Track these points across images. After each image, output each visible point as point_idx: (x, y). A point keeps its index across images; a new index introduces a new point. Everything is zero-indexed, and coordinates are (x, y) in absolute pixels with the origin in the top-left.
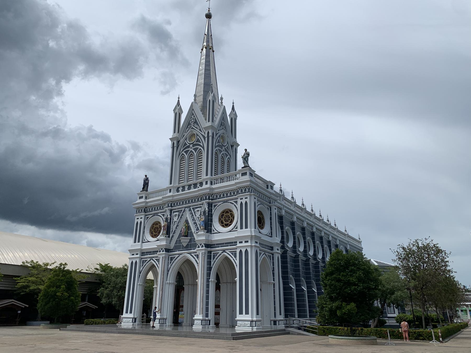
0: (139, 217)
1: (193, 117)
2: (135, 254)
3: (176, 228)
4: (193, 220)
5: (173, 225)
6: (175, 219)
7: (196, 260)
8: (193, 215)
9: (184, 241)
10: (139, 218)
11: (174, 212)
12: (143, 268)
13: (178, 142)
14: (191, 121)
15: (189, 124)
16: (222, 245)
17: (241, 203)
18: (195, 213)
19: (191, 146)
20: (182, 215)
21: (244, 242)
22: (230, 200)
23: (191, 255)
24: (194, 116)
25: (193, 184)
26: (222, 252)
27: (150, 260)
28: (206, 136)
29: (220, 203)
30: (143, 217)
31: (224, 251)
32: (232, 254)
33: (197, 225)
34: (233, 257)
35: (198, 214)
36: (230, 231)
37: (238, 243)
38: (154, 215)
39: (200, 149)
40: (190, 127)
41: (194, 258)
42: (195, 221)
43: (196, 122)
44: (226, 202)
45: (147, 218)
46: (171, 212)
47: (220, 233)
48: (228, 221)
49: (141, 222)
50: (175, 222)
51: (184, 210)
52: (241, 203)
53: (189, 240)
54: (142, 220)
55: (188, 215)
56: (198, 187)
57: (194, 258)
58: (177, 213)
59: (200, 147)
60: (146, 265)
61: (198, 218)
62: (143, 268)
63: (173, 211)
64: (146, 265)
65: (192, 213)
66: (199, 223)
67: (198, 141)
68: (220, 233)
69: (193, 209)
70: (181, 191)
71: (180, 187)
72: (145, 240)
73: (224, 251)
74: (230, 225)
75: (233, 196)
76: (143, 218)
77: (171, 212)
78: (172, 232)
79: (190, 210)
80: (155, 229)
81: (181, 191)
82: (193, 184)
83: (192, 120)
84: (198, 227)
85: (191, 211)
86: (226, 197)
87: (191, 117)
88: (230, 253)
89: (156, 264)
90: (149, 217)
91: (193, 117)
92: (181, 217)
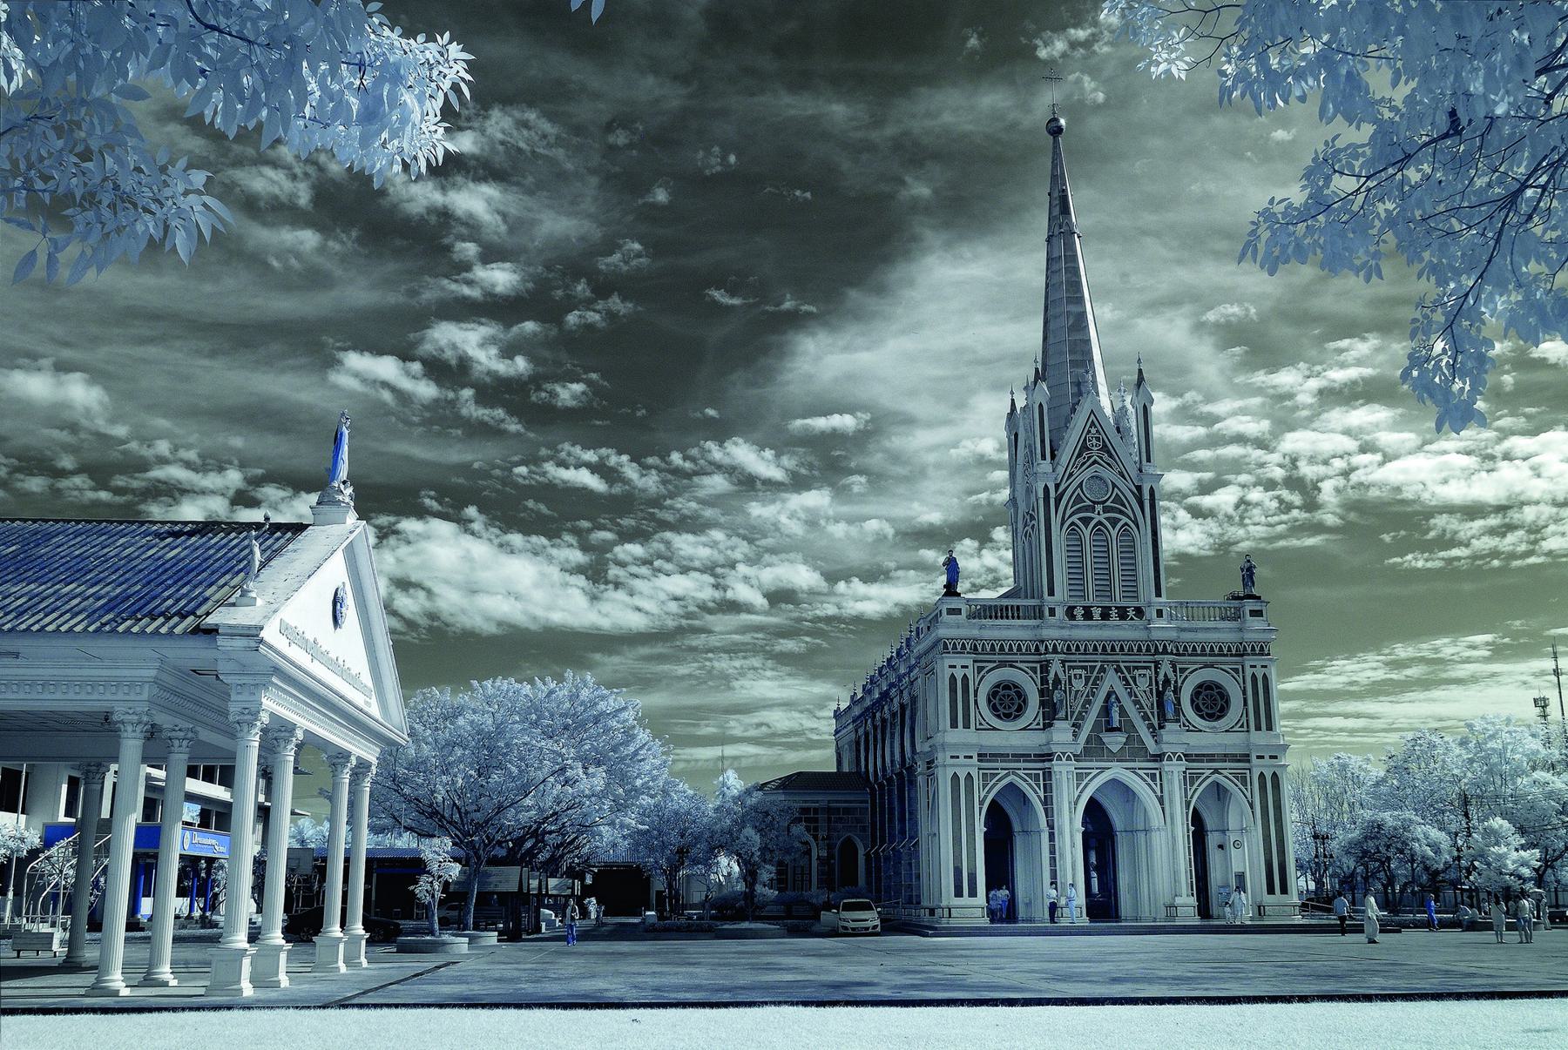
0: (959, 662)
1: (1093, 430)
2: (962, 758)
3: (1083, 706)
4: (1130, 694)
5: (1073, 697)
6: (1078, 685)
7: (1149, 785)
8: (1128, 683)
9: (1115, 741)
10: (959, 667)
11: (1070, 667)
12: (988, 792)
13: (1057, 486)
14: (1090, 441)
15: (1085, 448)
16: (1211, 758)
17: (1254, 677)
18: (1134, 679)
19: (1099, 508)
20: (1097, 678)
21: (1267, 757)
22: (1221, 663)
23: (1136, 774)
24: (1097, 431)
25: (1116, 608)
26: (1212, 773)
27: (1007, 775)
28: (1146, 496)
29: (1196, 666)
30: (970, 663)
31: (1216, 771)
32: (1237, 778)
33: (1142, 707)
34: (1239, 784)
35: (1143, 684)
36: (1226, 731)
37: (1253, 757)
38: (1002, 664)
39: (1126, 524)
40: (1089, 458)
41: (1145, 781)
42: (1136, 696)
43: (1105, 448)
44: (1212, 666)
45: (980, 669)
46: (1064, 666)
47: (1201, 731)
48: (1207, 708)
49: (965, 677)
50: (1077, 692)
51: (1103, 670)
52: (1254, 677)
53: (1125, 740)
54: (969, 673)
55: (1111, 681)
56: (1132, 619)
57: (1145, 781)
58: (1083, 673)
59: (1125, 520)
60: (995, 785)
61: (1145, 692)
62: (988, 792)
63: (1067, 664)
64: (995, 785)
65: (1125, 679)
66: (1149, 705)
67: (1117, 500)
68: (1201, 731)
69: (1128, 668)
70: (1079, 617)
71: (1075, 607)
72: (981, 724)
73: (1216, 771)
74: (1202, 717)
75: (1226, 655)
76: (971, 668)
77: (1064, 666)
78: (1073, 713)
79: (1118, 670)
80: (1000, 699)
81: (1079, 617)
82: (1116, 608)
83: (1094, 441)
84: (1145, 713)
85: (1123, 673)
86: (1210, 655)
87: (1089, 432)
88: (1230, 776)
89: (1030, 785)
90: (984, 667)
91: (1093, 430)
92: (1094, 683)
